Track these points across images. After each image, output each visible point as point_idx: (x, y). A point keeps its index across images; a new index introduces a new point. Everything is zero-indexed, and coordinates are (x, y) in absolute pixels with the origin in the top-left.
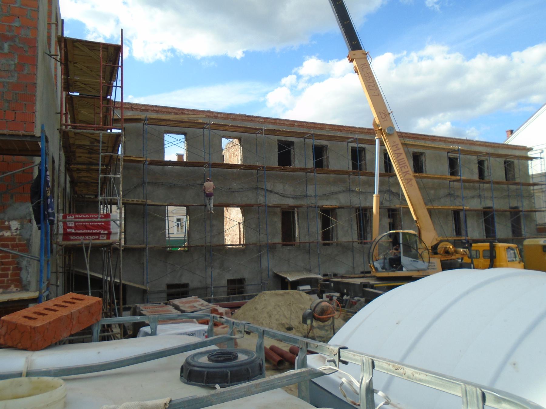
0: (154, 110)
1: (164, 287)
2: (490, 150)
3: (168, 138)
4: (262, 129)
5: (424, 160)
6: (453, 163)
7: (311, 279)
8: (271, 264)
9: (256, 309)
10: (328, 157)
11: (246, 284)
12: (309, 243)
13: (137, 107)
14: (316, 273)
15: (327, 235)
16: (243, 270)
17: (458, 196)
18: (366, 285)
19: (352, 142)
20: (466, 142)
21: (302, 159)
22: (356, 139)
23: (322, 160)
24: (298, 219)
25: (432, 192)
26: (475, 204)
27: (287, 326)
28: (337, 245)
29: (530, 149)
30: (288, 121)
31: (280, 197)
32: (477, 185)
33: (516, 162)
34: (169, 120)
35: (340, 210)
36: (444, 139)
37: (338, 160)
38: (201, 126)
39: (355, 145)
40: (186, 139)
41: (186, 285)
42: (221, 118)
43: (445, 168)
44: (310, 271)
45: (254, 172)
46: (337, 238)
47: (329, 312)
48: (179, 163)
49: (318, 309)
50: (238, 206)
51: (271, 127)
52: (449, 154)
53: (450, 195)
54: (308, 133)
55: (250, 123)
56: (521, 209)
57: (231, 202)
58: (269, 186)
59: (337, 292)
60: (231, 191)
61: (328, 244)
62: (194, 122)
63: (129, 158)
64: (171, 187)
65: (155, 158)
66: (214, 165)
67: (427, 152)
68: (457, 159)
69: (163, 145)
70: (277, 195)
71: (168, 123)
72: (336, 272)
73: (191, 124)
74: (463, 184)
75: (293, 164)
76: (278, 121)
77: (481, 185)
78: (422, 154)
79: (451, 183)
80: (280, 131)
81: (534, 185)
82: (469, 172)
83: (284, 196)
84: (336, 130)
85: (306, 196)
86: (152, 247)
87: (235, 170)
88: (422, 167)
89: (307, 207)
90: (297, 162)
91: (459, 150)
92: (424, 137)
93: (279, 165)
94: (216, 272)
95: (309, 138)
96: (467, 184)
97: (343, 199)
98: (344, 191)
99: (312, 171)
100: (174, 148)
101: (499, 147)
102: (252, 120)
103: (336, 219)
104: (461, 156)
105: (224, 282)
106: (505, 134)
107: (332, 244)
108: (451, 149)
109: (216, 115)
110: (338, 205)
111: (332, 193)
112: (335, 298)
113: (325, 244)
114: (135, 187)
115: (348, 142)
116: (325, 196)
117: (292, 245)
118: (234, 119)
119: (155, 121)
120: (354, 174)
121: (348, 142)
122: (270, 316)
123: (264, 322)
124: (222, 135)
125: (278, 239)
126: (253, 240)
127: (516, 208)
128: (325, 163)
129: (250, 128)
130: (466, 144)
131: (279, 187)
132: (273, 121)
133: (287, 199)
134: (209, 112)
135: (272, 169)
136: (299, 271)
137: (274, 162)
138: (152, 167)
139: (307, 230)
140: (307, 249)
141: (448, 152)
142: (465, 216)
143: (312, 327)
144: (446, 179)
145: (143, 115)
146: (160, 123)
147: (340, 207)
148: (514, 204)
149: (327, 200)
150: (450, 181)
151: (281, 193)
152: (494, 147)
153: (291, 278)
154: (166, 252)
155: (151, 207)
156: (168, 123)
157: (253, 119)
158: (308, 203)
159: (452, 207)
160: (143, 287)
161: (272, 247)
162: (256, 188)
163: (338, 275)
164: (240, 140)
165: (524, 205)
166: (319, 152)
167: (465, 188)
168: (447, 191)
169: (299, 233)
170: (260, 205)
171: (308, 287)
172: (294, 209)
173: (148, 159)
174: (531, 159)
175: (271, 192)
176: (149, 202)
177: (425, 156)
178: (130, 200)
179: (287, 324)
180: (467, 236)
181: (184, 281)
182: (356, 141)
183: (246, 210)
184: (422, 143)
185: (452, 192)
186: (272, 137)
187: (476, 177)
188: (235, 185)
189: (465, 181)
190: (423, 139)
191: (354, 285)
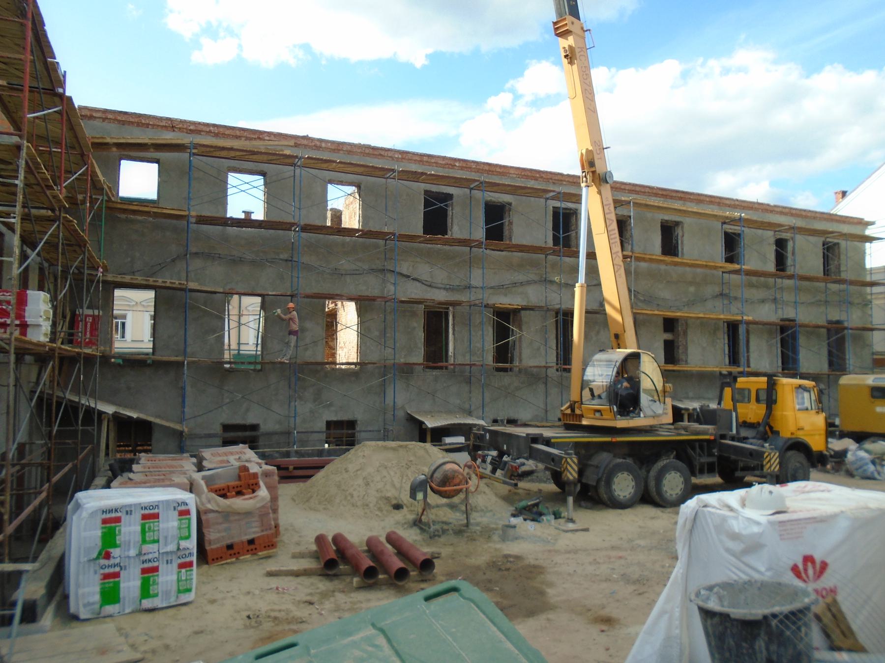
0: (210, 132)
1: (218, 429)
2: (799, 223)
3: (233, 179)
4: (393, 171)
5: (680, 234)
6: (731, 242)
7: (470, 427)
8: (403, 398)
9: (347, 471)
10: (511, 223)
11: (358, 429)
12: (471, 365)
13: (181, 126)
14: (478, 418)
15: (503, 354)
16: (354, 406)
17: (736, 298)
18: (535, 439)
19: (553, 198)
20: (756, 206)
21: (468, 224)
22: (559, 193)
24: (454, 325)
25: (692, 289)
26: (767, 313)
27: (394, 502)
28: (520, 371)
29: (869, 224)
30: (444, 158)
31: (425, 287)
32: (771, 280)
33: (843, 244)
34: (231, 149)
35: (528, 312)
36: (718, 200)
37: (530, 228)
38: (289, 161)
39: (557, 204)
40: (266, 184)
41: (254, 427)
43: (718, 249)
44: (470, 413)
45: (382, 242)
46: (521, 360)
47: (457, 481)
48: (247, 222)
49: (438, 475)
50: (350, 299)
51: (414, 167)
52: (725, 226)
53: (722, 295)
54: (475, 181)
55: (376, 160)
56: (846, 324)
57: (338, 292)
58: (405, 268)
59: (495, 449)
60: (338, 274)
61: (505, 370)
63: (159, 211)
64: (236, 262)
65: (207, 212)
66: (306, 228)
67: (687, 221)
68: (739, 235)
69: (225, 190)
71: (232, 154)
72: (513, 415)
73: (271, 157)
74: (744, 277)
75: (449, 232)
76: (425, 159)
77: (779, 281)
78: (677, 224)
80: (426, 174)
81: (873, 284)
82: (758, 257)
83: (430, 286)
84: (527, 177)
85: (469, 287)
86: (194, 362)
87: (348, 239)
88: (676, 247)
89: (470, 306)
90: (456, 230)
91: (740, 219)
92: (682, 195)
93: (426, 230)
94: (303, 408)
95: (477, 188)
96: (754, 279)
97: (534, 295)
98: (535, 282)
99: (479, 245)
100: (246, 197)
101: (815, 218)
102: (380, 155)
103: (520, 329)
104: (746, 230)
105: (321, 425)
106: (833, 196)
107: (511, 370)
108: (727, 218)
109: (318, 144)
110: (524, 304)
111: (514, 284)
112: (489, 459)
113: (499, 370)
114: (173, 261)
115: (547, 199)
116: (500, 288)
117: (441, 368)
118: (349, 152)
119: (208, 149)
120: (555, 253)
121: (547, 199)
122: (367, 484)
123: (355, 494)
124: (328, 178)
125: (418, 357)
126: (374, 357)
127: (838, 322)
128: (506, 233)
129: (373, 167)
130: (756, 209)
131: (423, 270)
132: (417, 158)
133: (437, 291)
134: (306, 138)
135: (411, 238)
136: (449, 412)
137: (417, 226)
139: (470, 344)
140: (466, 376)
142: (748, 332)
143: (426, 506)
144: (715, 268)
145: (186, 139)
146: (217, 154)
147: (525, 309)
148: (835, 315)
149: (506, 295)
150: (723, 272)
151: (428, 279)
152: (806, 217)
153: (431, 423)
154: (222, 373)
155: (199, 294)
156: (232, 154)
157: (383, 153)
158: (473, 298)
159: (722, 317)
160: (178, 427)
161: (406, 370)
163: (519, 423)
164: (359, 187)
165: (853, 319)
166: (495, 214)
167: (751, 285)
168: (717, 289)
169: (454, 349)
170: (386, 300)
171: (461, 440)
173: (193, 213)
174: (871, 239)
175: (408, 277)
176: (192, 285)
177: (682, 227)
178: (160, 280)
179: (396, 498)
180: (749, 367)
181: (251, 420)
182: (558, 197)
183: (364, 305)
184: (677, 205)
185: (726, 291)
186: (415, 185)
187: (771, 267)
188: (345, 264)
189: (749, 273)
190: (681, 199)
191: (518, 437)
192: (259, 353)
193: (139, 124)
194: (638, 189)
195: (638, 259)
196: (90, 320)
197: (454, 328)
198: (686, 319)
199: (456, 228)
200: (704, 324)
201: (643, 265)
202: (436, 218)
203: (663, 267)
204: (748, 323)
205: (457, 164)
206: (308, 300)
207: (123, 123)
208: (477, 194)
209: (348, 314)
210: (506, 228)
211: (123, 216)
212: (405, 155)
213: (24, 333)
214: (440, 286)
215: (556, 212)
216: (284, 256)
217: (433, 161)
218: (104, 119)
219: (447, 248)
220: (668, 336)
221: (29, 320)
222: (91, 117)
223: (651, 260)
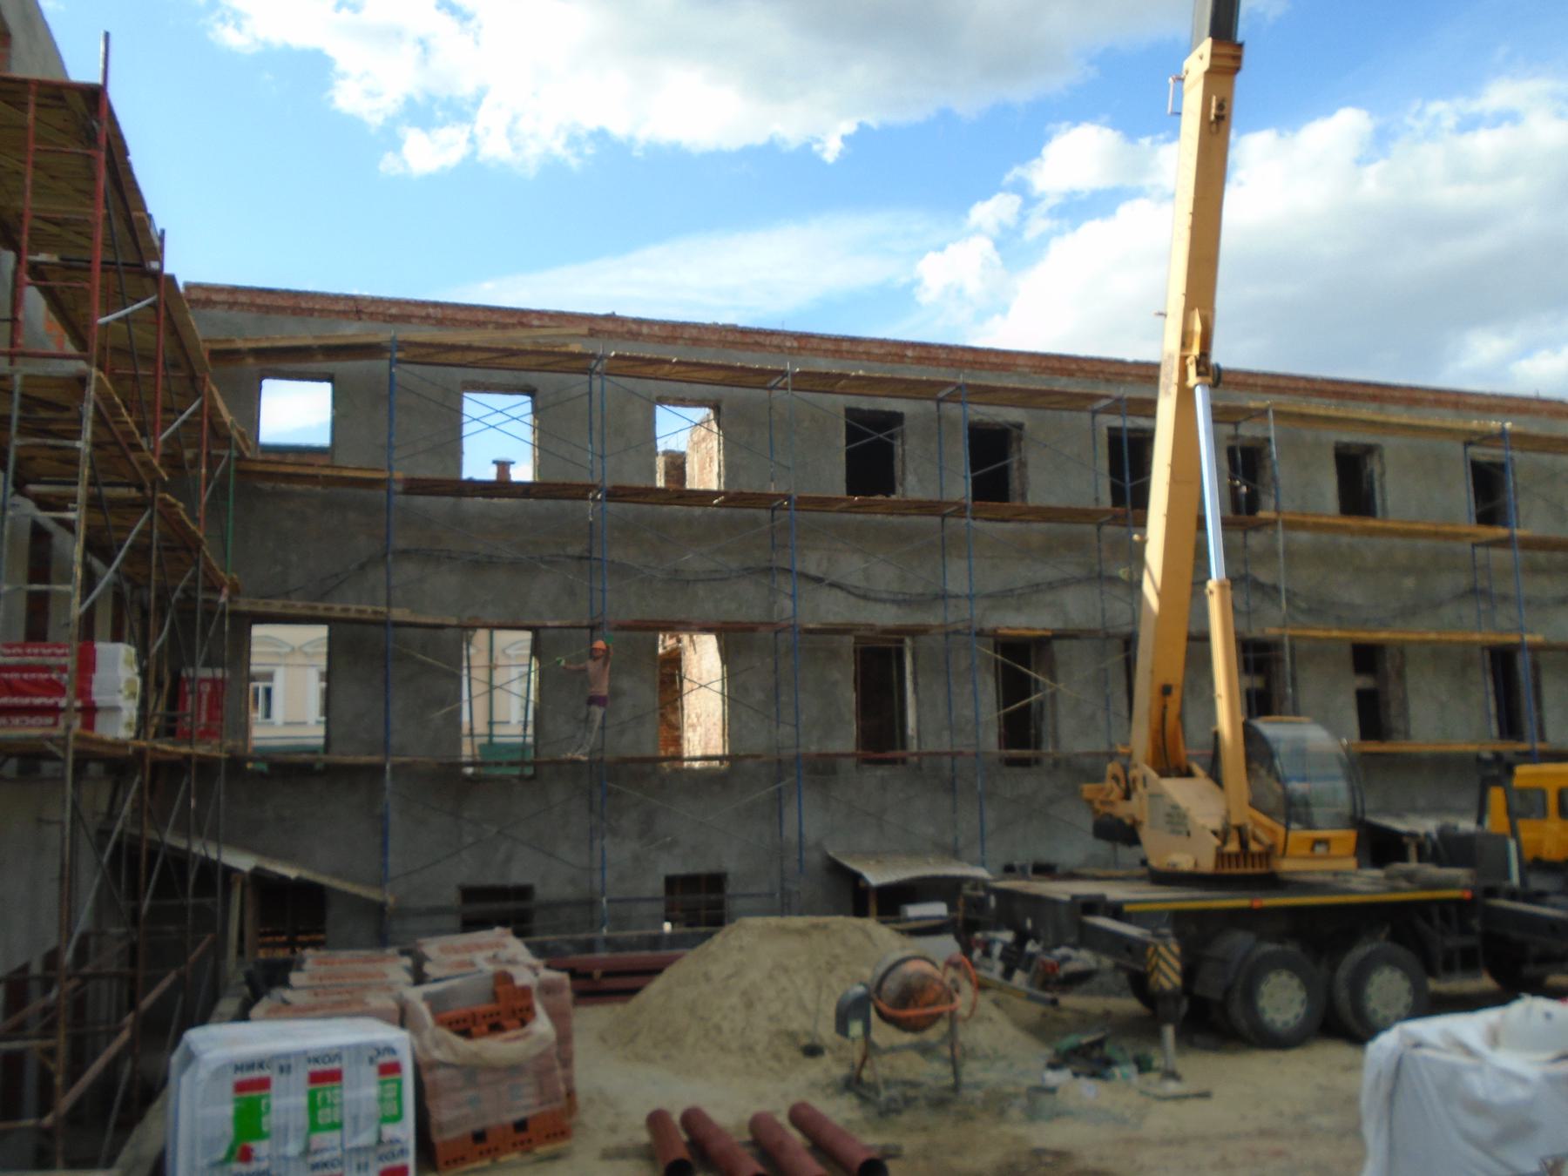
0: (428, 317)
1: (451, 897)
3: (475, 405)
4: (783, 374)
5: (1377, 469)
6: (1488, 484)
7: (956, 883)
8: (814, 824)
9: (707, 978)
10: (1023, 464)
11: (729, 891)
12: (954, 755)
13: (372, 309)
14: (973, 863)
15: (1021, 730)
16: (722, 846)
17: (1505, 598)
18: (1092, 905)
19: (1107, 410)
20: (1536, 406)
21: (933, 471)
22: (1119, 400)
23: (1003, 474)
25: (1409, 583)
27: (805, 1041)
28: (1056, 764)
31: (852, 599)
35: (1066, 643)
36: (1453, 398)
37: (1060, 474)
38: (581, 364)
39: (1117, 422)
40: (536, 411)
41: (524, 892)
42: (651, 337)
43: (1461, 498)
44: (955, 854)
45: (764, 514)
46: (1056, 742)
47: (930, 996)
48: (502, 487)
49: (892, 985)
50: (706, 629)
51: (823, 365)
52: (1472, 450)
53: (1474, 592)
54: (945, 384)
55: (749, 354)
57: (682, 616)
58: (812, 563)
59: (1009, 927)
60: (680, 581)
61: (1024, 763)
62: (553, 353)
63: (335, 473)
64: (480, 564)
65: (428, 470)
66: (617, 494)
67: (1389, 443)
68: (1502, 467)
69: (458, 426)
70: (840, 594)
71: (471, 357)
72: (1045, 855)
73: (543, 360)
74: (1519, 554)
75: (899, 489)
76: (845, 346)
78: (1369, 450)
79: (1480, 552)
80: (847, 376)
83: (865, 597)
84: (1053, 371)
85: (943, 597)
86: (403, 765)
87: (698, 511)
88: (1370, 496)
89: (947, 635)
90: (913, 484)
91: (1503, 434)
92: (1377, 392)
93: (851, 490)
94: (619, 852)
95: (950, 398)
96: (1541, 557)
97: (1079, 607)
98: (1079, 581)
99: (960, 511)
100: (498, 437)
102: (757, 344)
103: (1053, 678)
104: (1517, 455)
105: (656, 886)
107: (1038, 761)
108: (1474, 433)
109: (634, 327)
110: (1058, 625)
111: (1036, 588)
112: (997, 950)
113: (1011, 762)
114: (362, 567)
115: (1095, 413)
116: (1005, 597)
117: (893, 762)
119: (423, 351)
120: (1116, 520)
122: (749, 1005)
123: (726, 1026)
124: (655, 395)
125: (845, 741)
126: (758, 741)
128: (1015, 484)
129: (742, 368)
130: (1536, 412)
131: (851, 567)
132: (830, 346)
133: (879, 607)
134: (611, 318)
135: (823, 504)
136: (914, 853)
137: (832, 478)
138: (420, 501)
139: (949, 712)
140: (943, 777)
141: (1468, 444)
142: (1536, 667)
143: (870, 1049)
144: (1456, 536)
145: (383, 334)
146: (443, 358)
149: (1019, 609)
150: (1474, 545)
151: (856, 585)
153: (876, 876)
154: (457, 785)
155: (411, 631)
156: (471, 357)
157: (761, 339)
158: (951, 619)
159: (1477, 637)
160: (374, 894)
161: (823, 769)
162: (768, 571)
163: (1059, 870)
164: (716, 408)
167: (1534, 570)
168: (1464, 581)
169: (919, 721)
170: (777, 629)
171: (938, 909)
172: (902, 641)
173: (399, 475)
175: (819, 580)
176: (398, 614)
177: (1381, 457)
178: (338, 607)
179: (807, 1033)
180: (1542, 738)
181: (516, 877)
182: (1118, 407)
184: (1366, 412)
185: (1482, 583)
188: (693, 560)
189: (1528, 544)
190: (1374, 398)
191: (1055, 903)
192: (530, 740)
193: (297, 311)
194: (1282, 383)
195: (1290, 526)
196: (207, 688)
197: (915, 684)
198: (1402, 648)
199: (911, 480)
200: (1438, 653)
201: (1303, 537)
203: (1345, 540)
204: (1535, 649)
205: (909, 353)
206: (624, 634)
207: (267, 309)
208: (952, 410)
209: (703, 659)
211: (267, 486)
212: (805, 342)
213: (89, 725)
214: (885, 596)
215: (1115, 437)
216: (576, 549)
217: (861, 349)
218: (232, 305)
219: (894, 520)
220: (1365, 682)
221: (100, 698)
222: (208, 303)
223: (1318, 527)
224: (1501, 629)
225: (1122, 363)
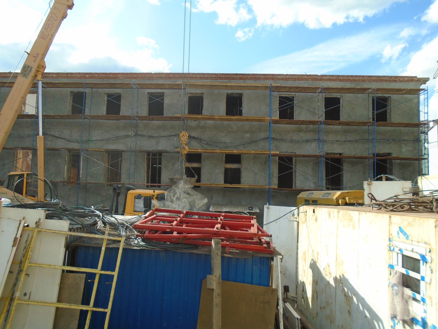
2: (348, 85)
21: (97, 107)
25: (248, 135)
26: (311, 149)
30: (79, 73)
33: (394, 97)
56: (394, 155)
70: (63, 140)
76: (69, 75)
83: (69, 141)
92: (241, 76)
101: (363, 81)
131: (66, 133)
132: (65, 76)
152: (354, 80)
190: (241, 79)
202: (286, 109)
203: (225, 123)
205: (87, 76)
210: (388, 111)
212: (92, 75)
214: (75, 141)
217: (74, 76)
224: (286, 149)
225: (363, 76)
